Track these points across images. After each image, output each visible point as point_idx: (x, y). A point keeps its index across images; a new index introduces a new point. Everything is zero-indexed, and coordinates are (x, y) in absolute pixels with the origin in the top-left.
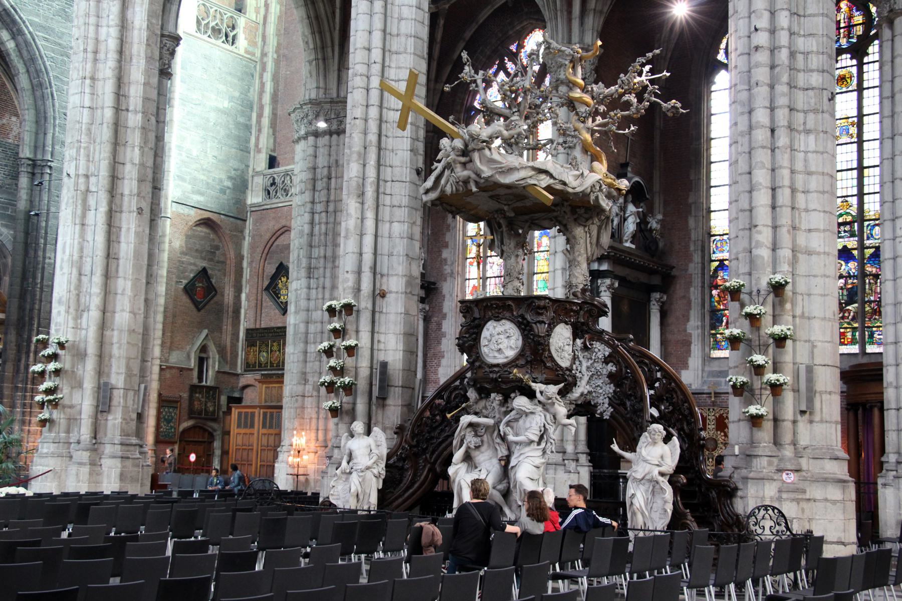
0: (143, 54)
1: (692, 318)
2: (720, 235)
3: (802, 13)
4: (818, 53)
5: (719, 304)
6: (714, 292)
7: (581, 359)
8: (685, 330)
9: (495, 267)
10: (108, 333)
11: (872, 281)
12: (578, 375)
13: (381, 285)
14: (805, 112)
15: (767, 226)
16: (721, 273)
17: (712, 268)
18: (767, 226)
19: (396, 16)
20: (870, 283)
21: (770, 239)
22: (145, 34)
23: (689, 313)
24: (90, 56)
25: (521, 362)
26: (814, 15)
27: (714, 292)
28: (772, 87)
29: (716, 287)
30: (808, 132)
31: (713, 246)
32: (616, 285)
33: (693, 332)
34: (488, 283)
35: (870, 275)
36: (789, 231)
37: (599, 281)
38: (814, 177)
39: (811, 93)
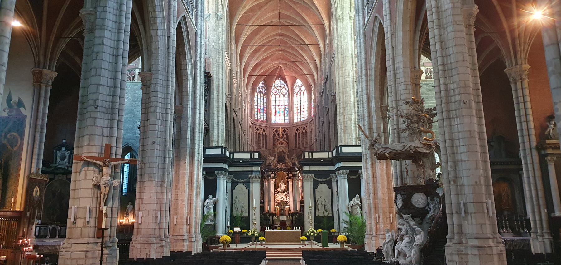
0: (375, 115)
3: (450, 75)
4: (457, 88)
7: (431, 204)
10: (376, 200)
12: (429, 210)
13: (405, 182)
14: (455, 110)
15: (444, 155)
18: (444, 155)
19: (400, 94)
21: (445, 159)
22: (375, 109)
24: (362, 119)
25: (403, 208)
26: (455, 75)
28: (441, 105)
30: (457, 117)
32: (555, 158)
36: (450, 156)
37: (546, 158)
38: (461, 133)
39: (456, 103)
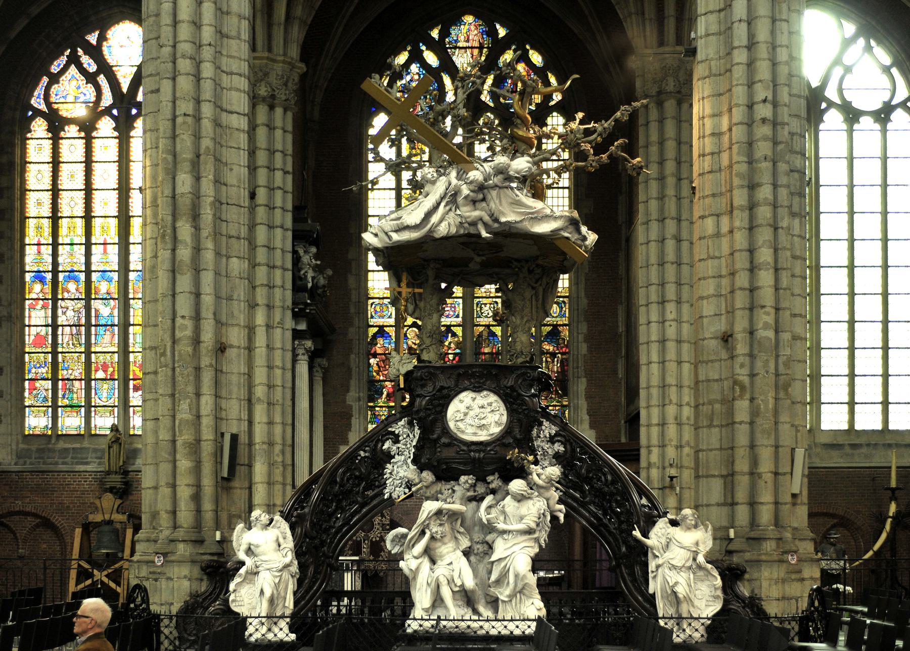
1: (352, 388)
2: (379, 298)
5: (378, 374)
6: (373, 361)
8: (344, 401)
9: (70, 313)
11: (549, 360)
16: (380, 341)
17: (370, 334)
20: (546, 361)
23: (349, 382)
27: (373, 361)
29: (375, 355)
31: (371, 310)
33: (353, 404)
34: (60, 332)
35: (547, 353)
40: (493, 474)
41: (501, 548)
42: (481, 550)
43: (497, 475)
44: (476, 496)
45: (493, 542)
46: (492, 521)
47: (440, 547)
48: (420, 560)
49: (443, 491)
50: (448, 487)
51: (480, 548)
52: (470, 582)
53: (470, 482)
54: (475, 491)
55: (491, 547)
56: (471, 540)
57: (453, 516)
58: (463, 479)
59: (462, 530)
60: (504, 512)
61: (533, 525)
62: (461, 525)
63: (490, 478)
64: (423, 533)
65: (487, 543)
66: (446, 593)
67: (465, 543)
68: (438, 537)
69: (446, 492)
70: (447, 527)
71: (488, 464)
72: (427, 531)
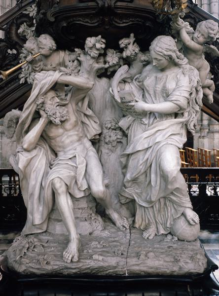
40: (128, 37)
41: (141, 138)
42: (114, 138)
43: (132, 39)
44: (106, 69)
45: (128, 128)
46: (128, 98)
47: (62, 135)
48: (34, 152)
49: (67, 63)
50: (73, 57)
51: (114, 136)
52: (98, 188)
53: (98, 46)
54: (105, 62)
55: (125, 135)
56: (101, 126)
57: (79, 93)
58: (90, 41)
59: (89, 112)
60: (143, 89)
61: (183, 102)
62: (89, 106)
63: (123, 42)
64: (37, 116)
65: (121, 129)
66: (64, 202)
67: (94, 129)
68: (57, 121)
69: (70, 64)
70: (71, 108)
71: (122, 17)
72: (42, 112)
